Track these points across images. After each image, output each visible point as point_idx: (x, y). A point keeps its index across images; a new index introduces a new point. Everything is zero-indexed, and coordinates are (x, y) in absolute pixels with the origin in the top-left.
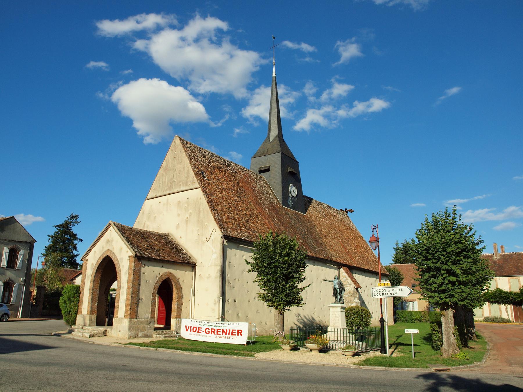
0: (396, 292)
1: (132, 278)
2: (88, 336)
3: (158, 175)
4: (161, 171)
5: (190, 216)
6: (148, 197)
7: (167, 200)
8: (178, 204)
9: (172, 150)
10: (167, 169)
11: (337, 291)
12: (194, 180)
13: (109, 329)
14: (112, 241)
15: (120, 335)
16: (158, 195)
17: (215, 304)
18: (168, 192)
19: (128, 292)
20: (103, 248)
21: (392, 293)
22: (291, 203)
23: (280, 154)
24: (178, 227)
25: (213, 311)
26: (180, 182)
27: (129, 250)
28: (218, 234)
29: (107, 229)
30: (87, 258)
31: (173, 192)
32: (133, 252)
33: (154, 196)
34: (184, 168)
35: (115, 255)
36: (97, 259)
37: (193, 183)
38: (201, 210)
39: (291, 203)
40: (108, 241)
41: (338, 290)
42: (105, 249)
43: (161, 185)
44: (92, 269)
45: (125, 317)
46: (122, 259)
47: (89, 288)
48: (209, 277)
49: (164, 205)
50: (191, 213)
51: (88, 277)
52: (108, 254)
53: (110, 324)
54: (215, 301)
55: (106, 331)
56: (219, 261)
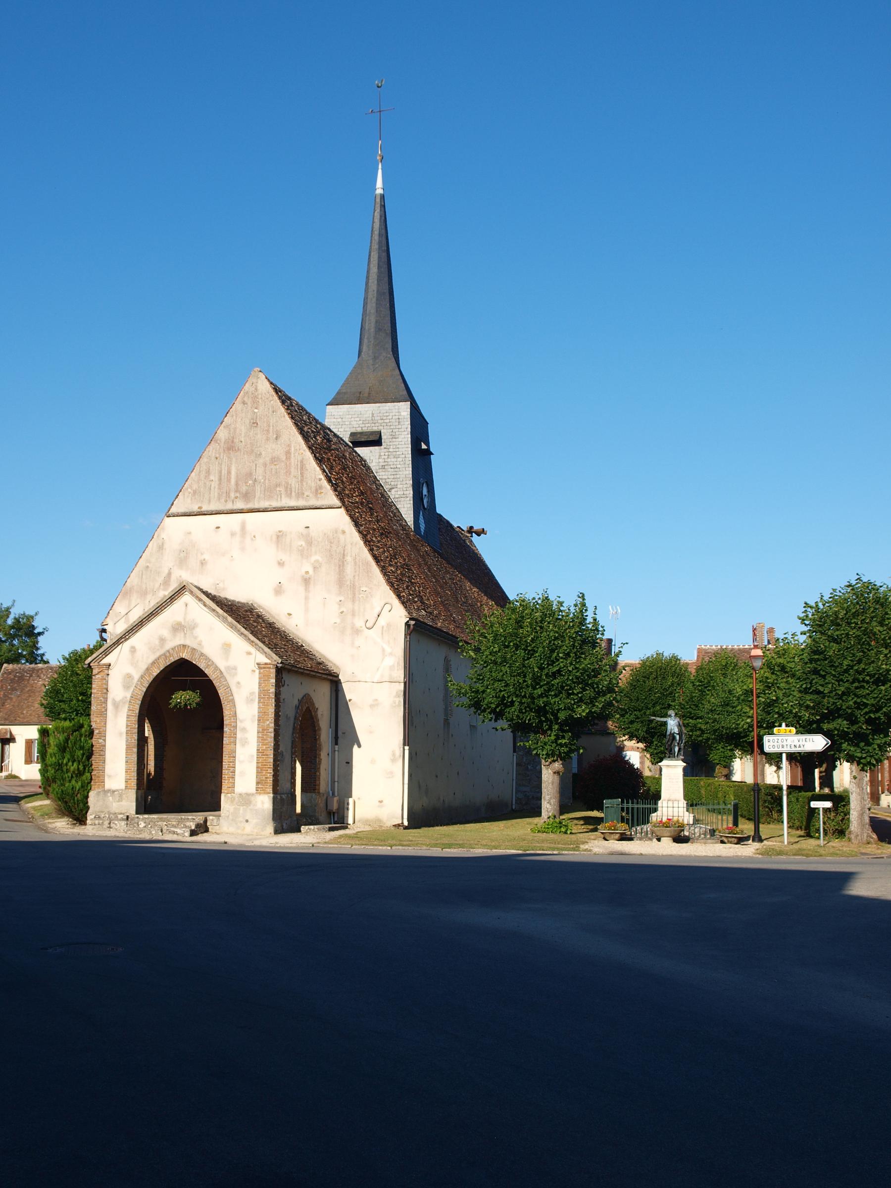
0: (804, 743)
1: (271, 710)
2: (187, 834)
3: (204, 460)
4: (212, 450)
5: (315, 568)
6: (174, 510)
8: (278, 537)
9: (244, 403)
10: (231, 447)
11: (674, 738)
12: (321, 487)
13: (211, 817)
14: (193, 627)
15: (248, 828)
16: (205, 508)
17: (394, 760)
18: (240, 505)
19: (261, 739)
20: (162, 640)
21: (798, 744)
23: (404, 409)
24: (279, 590)
27: (252, 650)
28: (397, 616)
29: (172, 598)
30: (106, 661)
31: (256, 506)
33: (195, 509)
34: (288, 453)
35: (207, 659)
36: (144, 667)
37: (318, 491)
38: (349, 558)
40: (178, 628)
41: (678, 737)
42: (169, 645)
43: (215, 484)
44: (126, 687)
47: (124, 730)
48: (375, 705)
49: (233, 534)
50: (317, 561)
51: (116, 706)
52: (185, 655)
53: (215, 806)
54: (394, 755)
55: (206, 821)
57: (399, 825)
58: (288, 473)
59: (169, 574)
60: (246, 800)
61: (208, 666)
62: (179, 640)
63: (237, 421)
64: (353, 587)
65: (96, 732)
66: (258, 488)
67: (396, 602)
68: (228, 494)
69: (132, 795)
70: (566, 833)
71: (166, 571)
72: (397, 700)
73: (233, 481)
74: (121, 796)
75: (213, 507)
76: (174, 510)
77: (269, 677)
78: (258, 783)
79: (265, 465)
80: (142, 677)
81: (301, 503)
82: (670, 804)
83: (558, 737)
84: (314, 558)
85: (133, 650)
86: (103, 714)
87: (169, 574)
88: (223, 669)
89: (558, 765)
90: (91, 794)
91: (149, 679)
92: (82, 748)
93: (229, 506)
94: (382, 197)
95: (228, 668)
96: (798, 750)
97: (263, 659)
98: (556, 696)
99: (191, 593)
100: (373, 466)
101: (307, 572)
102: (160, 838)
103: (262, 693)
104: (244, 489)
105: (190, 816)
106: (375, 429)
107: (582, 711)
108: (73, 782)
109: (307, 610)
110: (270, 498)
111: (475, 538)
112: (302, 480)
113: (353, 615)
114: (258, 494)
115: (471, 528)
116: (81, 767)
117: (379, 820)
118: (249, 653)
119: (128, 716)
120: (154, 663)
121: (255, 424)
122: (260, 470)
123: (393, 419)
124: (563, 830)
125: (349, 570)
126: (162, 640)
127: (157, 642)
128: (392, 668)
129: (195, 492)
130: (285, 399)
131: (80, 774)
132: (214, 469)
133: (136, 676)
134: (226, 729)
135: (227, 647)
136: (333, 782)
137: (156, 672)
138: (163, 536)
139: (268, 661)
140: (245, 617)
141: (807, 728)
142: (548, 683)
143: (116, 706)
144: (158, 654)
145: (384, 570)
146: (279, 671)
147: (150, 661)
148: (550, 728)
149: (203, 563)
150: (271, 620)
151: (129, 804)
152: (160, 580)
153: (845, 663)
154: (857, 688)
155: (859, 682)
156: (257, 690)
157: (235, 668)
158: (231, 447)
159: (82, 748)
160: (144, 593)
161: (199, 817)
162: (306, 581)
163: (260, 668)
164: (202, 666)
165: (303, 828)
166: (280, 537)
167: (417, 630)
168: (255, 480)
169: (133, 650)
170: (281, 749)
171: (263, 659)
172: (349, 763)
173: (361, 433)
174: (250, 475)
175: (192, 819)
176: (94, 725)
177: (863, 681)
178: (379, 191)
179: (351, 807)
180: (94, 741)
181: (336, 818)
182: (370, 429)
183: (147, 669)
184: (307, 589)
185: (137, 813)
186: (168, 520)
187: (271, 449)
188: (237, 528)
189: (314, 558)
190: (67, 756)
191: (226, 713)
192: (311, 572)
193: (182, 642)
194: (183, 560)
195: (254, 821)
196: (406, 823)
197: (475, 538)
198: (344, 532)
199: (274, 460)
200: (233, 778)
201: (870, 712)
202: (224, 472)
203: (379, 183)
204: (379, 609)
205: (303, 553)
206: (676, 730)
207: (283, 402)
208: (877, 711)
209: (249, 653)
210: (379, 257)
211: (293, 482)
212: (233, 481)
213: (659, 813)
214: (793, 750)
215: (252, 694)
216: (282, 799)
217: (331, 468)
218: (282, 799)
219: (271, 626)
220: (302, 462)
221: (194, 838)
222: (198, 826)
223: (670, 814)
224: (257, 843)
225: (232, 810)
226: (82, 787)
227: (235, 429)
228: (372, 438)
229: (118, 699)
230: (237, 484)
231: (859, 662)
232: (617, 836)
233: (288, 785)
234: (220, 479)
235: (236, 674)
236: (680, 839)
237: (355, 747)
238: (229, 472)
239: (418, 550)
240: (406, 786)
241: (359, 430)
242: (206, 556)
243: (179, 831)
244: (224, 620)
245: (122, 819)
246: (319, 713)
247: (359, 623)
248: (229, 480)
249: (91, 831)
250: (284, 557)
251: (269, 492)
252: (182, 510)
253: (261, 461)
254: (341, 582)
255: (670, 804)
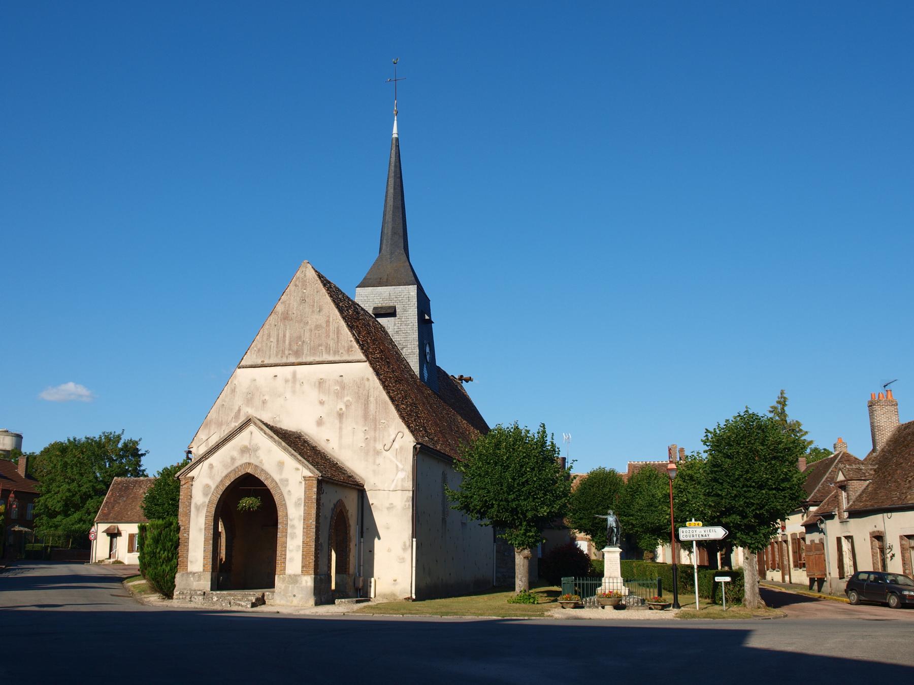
1: (314, 511)
2: (249, 606)
3: (266, 326)
4: (272, 319)
5: (347, 406)
6: (243, 363)
7: (294, 375)
8: (320, 383)
9: (296, 285)
11: (613, 531)
12: (352, 347)
13: (267, 593)
14: (256, 449)
15: (295, 601)
16: (266, 362)
17: (404, 549)
18: (292, 359)
20: (233, 459)
22: (426, 375)
23: (412, 290)
24: (320, 422)
25: (402, 560)
26: (320, 345)
27: (300, 467)
28: (408, 441)
29: (241, 428)
30: (191, 475)
31: (304, 360)
32: (317, 472)
33: (259, 362)
35: (267, 473)
36: (219, 479)
37: (349, 349)
38: (372, 399)
39: (426, 375)
40: (245, 450)
42: (238, 463)
43: (274, 345)
44: (205, 495)
45: (304, 571)
46: (286, 481)
47: (203, 526)
48: (391, 507)
49: (287, 381)
51: (198, 509)
52: (249, 471)
54: (405, 545)
55: (263, 596)
56: (411, 483)
57: (409, 598)
58: (328, 336)
59: (239, 410)
60: (294, 579)
61: (267, 479)
62: (245, 459)
63: (291, 299)
64: (375, 420)
65: (182, 528)
66: (305, 347)
67: (406, 431)
68: (283, 352)
69: (208, 576)
70: (533, 603)
71: (237, 408)
72: (407, 504)
73: (287, 342)
74: (199, 577)
75: (273, 361)
76: (243, 363)
77: (312, 487)
78: (303, 567)
79: (311, 330)
80: (217, 487)
81: (337, 358)
82: (611, 580)
83: (527, 531)
84: (346, 399)
85: (211, 466)
86: (188, 515)
87: (239, 410)
88: (278, 481)
89: (527, 552)
90: (178, 575)
91: (223, 488)
92: (171, 540)
93: (284, 360)
94: (397, 139)
95: (281, 480)
96: (704, 538)
97: (308, 473)
98: (525, 500)
99: (255, 424)
100: (390, 331)
101: (341, 409)
102: (229, 609)
103: (307, 498)
104: (295, 348)
105: (251, 592)
106: (392, 304)
107: (544, 511)
108: (164, 566)
109: (341, 437)
110: (314, 354)
111: (464, 384)
112: (338, 342)
113: (375, 441)
114: (305, 352)
115: (462, 376)
116: (170, 555)
117: (394, 595)
118: (297, 469)
119: (206, 517)
120: (226, 476)
121: (303, 301)
122: (307, 335)
123: (405, 297)
124: (532, 601)
125: (372, 407)
126: (233, 459)
127: (229, 461)
128: (403, 480)
129: (259, 350)
130: (326, 283)
131: (169, 560)
132: (274, 333)
133: (213, 486)
134: (279, 526)
135: (281, 465)
136: (359, 566)
137: (228, 483)
138: (235, 382)
139: (311, 475)
140: (295, 442)
141: (710, 522)
142: (519, 490)
143: (198, 509)
144: (229, 470)
145: (397, 408)
146: (320, 482)
147: (224, 475)
148: (521, 524)
149: (264, 402)
150: (314, 444)
151: (205, 583)
152: (233, 415)
153: (737, 473)
154: (745, 492)
155: (747, 487)
156: (303, 497)
157: (287, 480)
158: (286, 317)
159: (171, 540)
160: (220, 424)
161: (258, 593)
162: (341, 416)
163: (305, 480)
164: (262, 478)
165: (337, 601)
166: (321, 383)
167: (422, 452)
168: (304, 342)
169: (211, 466)
170: (321, 541)
171: (308, 473)
172: (371, 551)
173: (381, 308)
174: (299, 338)
175: (253, 595)
176: (180, 523)
177: (751, 486)
178: (395, 136)
179: (373, 584)
180: (180, 535)
181: (361, 593)
182: (387, 305)
183: (222, 481)
184: (341, 422)
185: (212, 590)
186: (239, 371)
187: (315, 319)
188: (290, 377)
189: (346, 399)
190: (160, 546)
191: (280, 514)
192: (344, 409)
193: (247, 461)
194: (249, 399)
195: (299, 596)
196: (414, 597)
197: (464, 384)
198: (368, 379)
199: (318, 327)
200: (285, 563)
201: (756, 509)
202: (281, 335)
203: (395, 130)
204: (393, 436)
205: (339, 395)
206: (614, 525)
207: (324, 285)
208: (761, 508)
209: (297, 469)
210: (395, 182)
211: (332, 343)
212: (287, 342)
213: (603, 587)
214: (701, 538)
215: (299, 499)
216: (321, 579)
217: (359, 333)
218: (321, 579)
219: (314, 449)
220: (338, 328)
221: (255, 609)
222: (257, 599)
223: (611, 588)
224: (302, 612)
225: (283, 587)
226: (171, 570)
227: (289, 304)
228: (389, 311)
229: (199, 503)
230: (290, 345)
231: (747, 472)
232: (572, 605)
233: (326, 568)
234: (278, 341)
235: (287, 485)
236: (618, 607)
237: (376, 539)
238: (284, 336)
239: (423, 393)
240: (414, 569)
241: (380, 305)
242: (267, 397)
243: (243, 604)
244: (279, 444)
245: (200, 595)
246: (349, 514)
247: (379, 446)
248: (284, 341)
249: (176, 603)
250: (324, 398)
251: (314, 350)
252: (249, 363)
253: (308, 327)
254: (366, 417)
255: (611, 580)
